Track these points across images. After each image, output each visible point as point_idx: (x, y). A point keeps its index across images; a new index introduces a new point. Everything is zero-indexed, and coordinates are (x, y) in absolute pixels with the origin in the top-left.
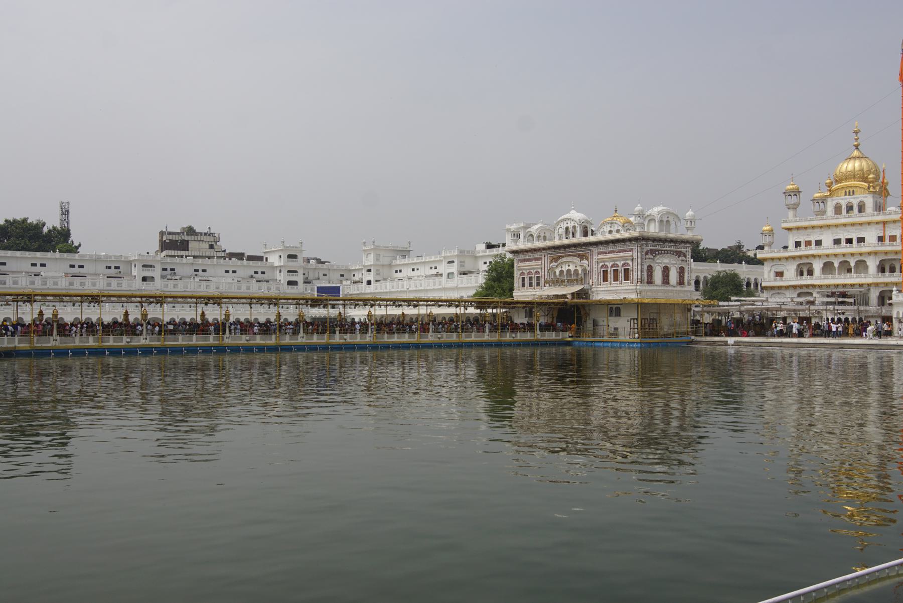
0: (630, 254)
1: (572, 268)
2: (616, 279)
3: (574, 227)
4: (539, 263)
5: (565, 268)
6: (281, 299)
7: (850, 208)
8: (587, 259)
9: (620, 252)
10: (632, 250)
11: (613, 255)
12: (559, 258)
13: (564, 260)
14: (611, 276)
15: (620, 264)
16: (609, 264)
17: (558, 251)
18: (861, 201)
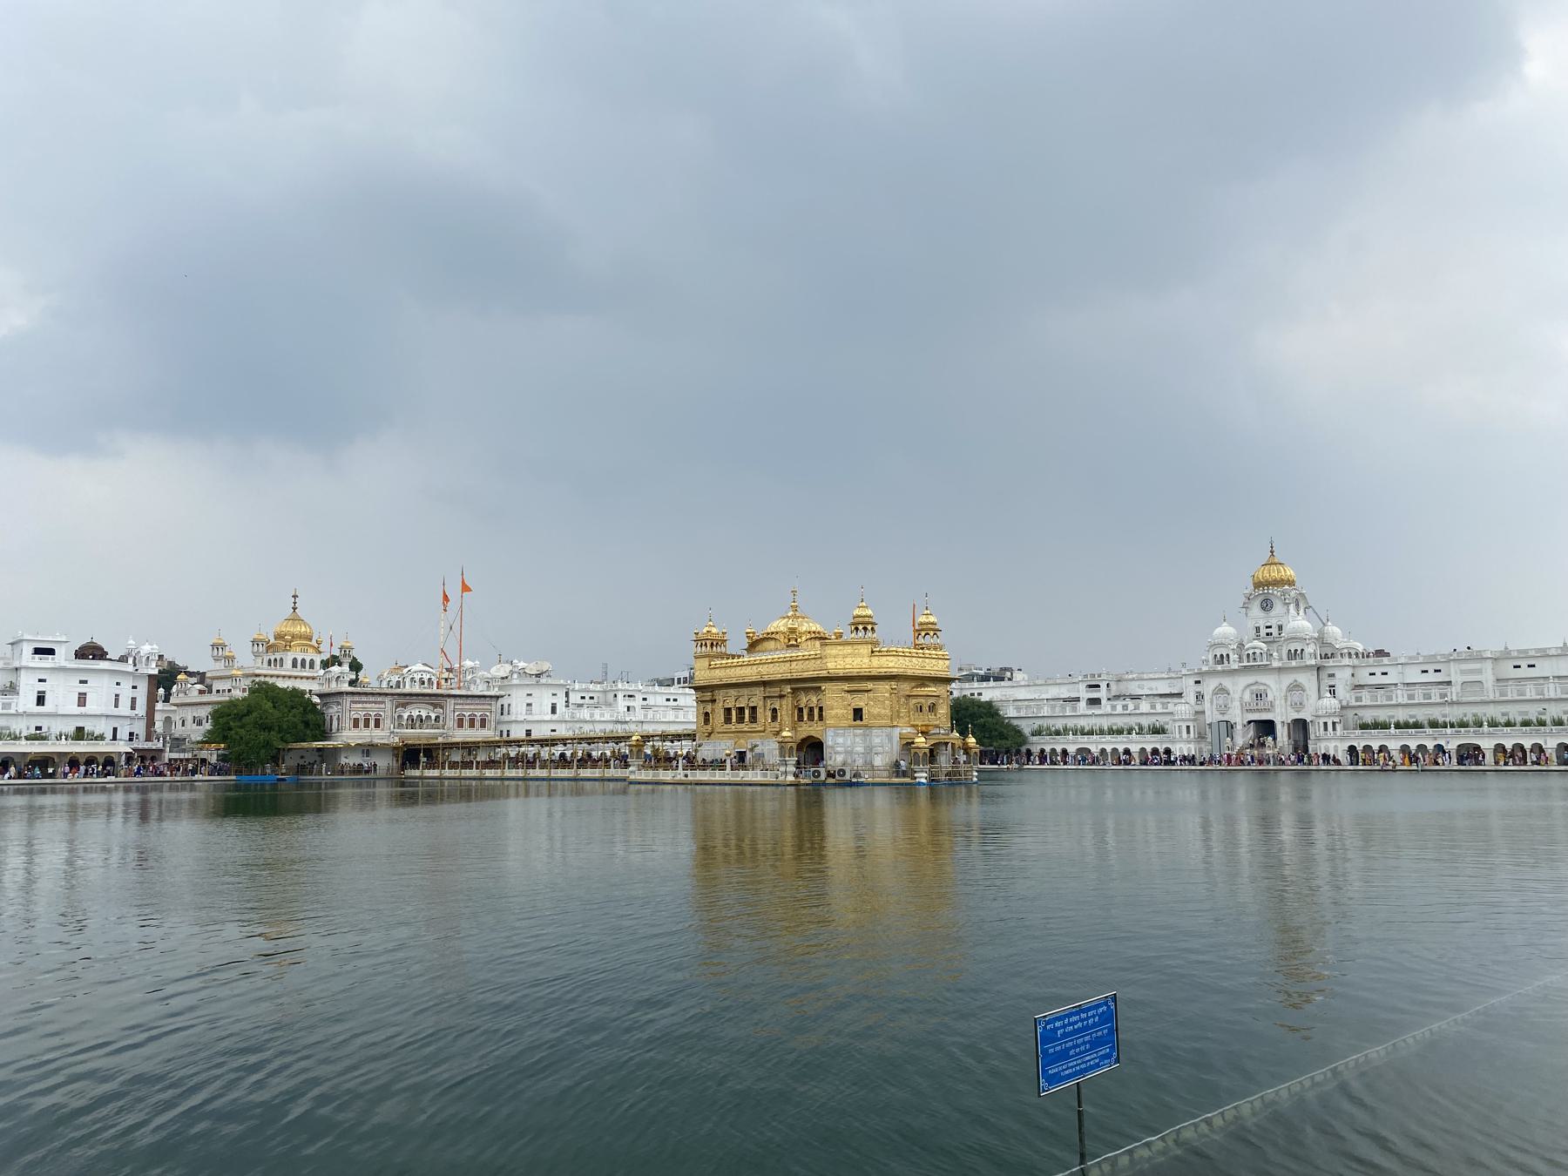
0: (489, 707)
1: (424, 714)
2: (472, 725)
3: (430, 679)
4: (383, 706)
5: (415, 713)
6: (567, 739)
7: (303, 661)
8: (442, 708)
9: (477, 704)
10: (490, 704)
11: (472, 707)
12: (408, 704)
13: (415, 705)
14: (466, 724)
15: (478, 714)
16: (467, 714)
17: (407, 699)
18: (312, 660)
